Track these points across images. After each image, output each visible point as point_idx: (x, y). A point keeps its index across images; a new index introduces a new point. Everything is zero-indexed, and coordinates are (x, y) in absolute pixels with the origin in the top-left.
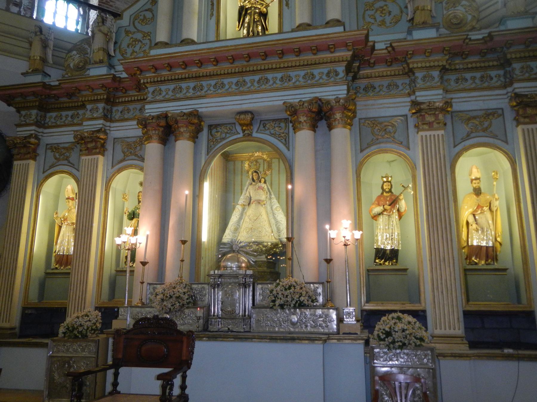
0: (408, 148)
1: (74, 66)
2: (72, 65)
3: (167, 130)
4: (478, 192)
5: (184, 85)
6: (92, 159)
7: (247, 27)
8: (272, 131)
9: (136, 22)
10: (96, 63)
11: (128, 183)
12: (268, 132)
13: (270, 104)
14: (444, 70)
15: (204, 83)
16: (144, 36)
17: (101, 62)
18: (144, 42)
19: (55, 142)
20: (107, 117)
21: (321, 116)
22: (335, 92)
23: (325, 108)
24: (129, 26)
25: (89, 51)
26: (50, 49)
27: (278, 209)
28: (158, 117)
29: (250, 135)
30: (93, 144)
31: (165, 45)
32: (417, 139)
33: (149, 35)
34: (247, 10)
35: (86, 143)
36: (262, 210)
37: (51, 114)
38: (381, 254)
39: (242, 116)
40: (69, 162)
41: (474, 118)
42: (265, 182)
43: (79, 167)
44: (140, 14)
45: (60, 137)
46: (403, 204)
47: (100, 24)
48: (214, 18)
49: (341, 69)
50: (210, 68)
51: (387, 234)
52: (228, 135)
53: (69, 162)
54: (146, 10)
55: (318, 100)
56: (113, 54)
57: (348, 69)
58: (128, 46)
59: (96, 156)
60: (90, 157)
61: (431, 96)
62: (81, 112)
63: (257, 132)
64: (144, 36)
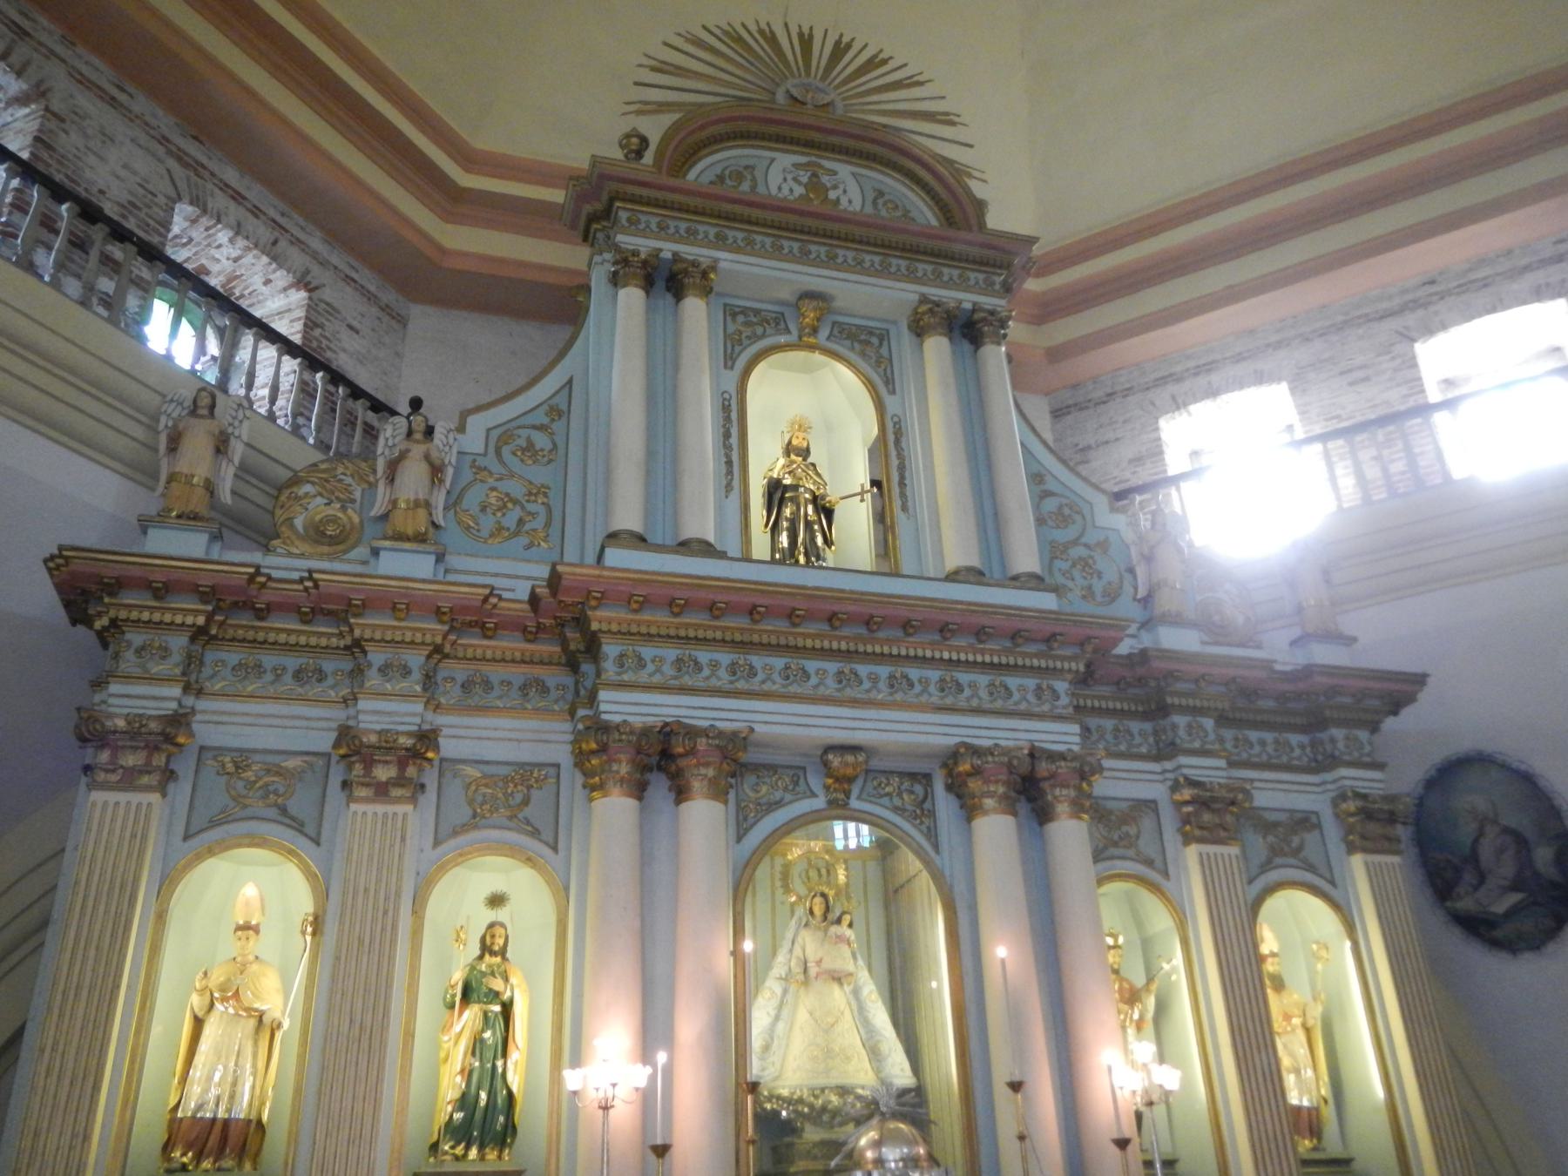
0: (1166, 874)
1: (305, 528)
2: (299, 523)
5: (704, 656)
6: (385, 815)
7: (788, 529)
8: (897, 802)
9: (506, 451)
10: (400, 537)
11: (482, 896)
12: (885, 801)
13: (922, 739)
15: (757, 661)
16: (530, 494)
17: (420, 538)
18: (531, 507)
19: (236, 743)
22: (1061, 736)
23: (1043, 768)
24: (485, 455)
25: (358, 495)
26: (231, 461)
27: (875, 996)
28: (646, 732)
29: (845, 805)
30: (388, 765)
31: (640, 541)
33: (545, 495)
34: (786, 488)
35: (369, 764)
37: (224, 655)
39: (850, 758)
40: (284, 811)
41: (1276, 825)
42: (850, 925)
43: (319, 833)
44: (520, 432)
45: (248, 730)
47: (418, 436)
48: (735, 495)
49: (1061, 686)
50: (773, 627)
52: (788, 797)
53: (284, 811)
54: (534, 427)
56: (440, 521)
58: (483, 509)
59: (402, 809)
60: (380, 809)
62: (328, 666)
63: (859, 798)
64: (530, 494)
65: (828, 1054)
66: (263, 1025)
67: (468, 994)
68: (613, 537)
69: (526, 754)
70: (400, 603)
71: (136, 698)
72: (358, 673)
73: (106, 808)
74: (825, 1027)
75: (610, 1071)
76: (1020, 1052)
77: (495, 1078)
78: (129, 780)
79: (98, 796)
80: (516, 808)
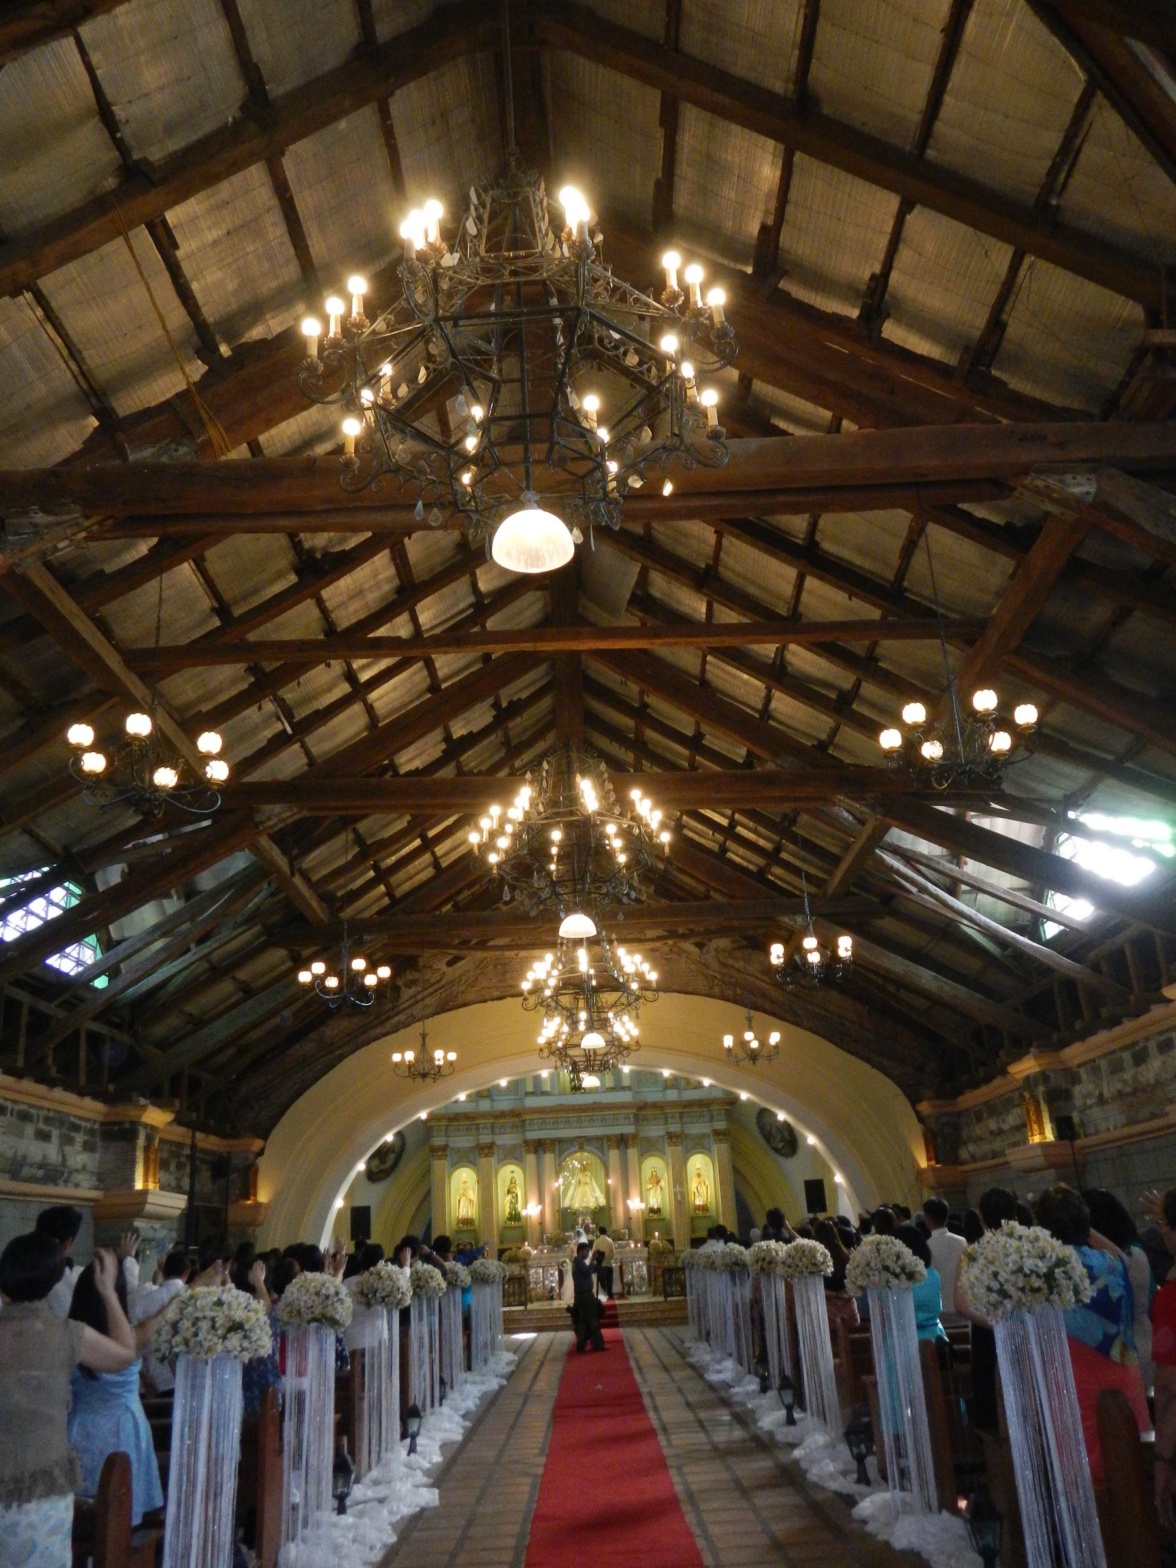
3: (539, 1147)
4: (699, 1175)
11: (509, 1173)
14: (681, 1113)
20: (493, 1133)
21: (622, 1142)
22: (629, 1129)
30: (487, 1150)
31: (533, 1094)
32: (669, 1150)
36: (587, 1187)
38: (652, 1210)
46: (662, 1183)
51: (655, 1200)
55: (622, 1135)
57: (636, 1116)
61: (675, 1128)
65: (582, 1201)
66: (471, 1201)
67: (509, 1192)
68: (527, 1094)
69: (513, 1142)
70: (484, 1115)
71: (438, 1141)
72: (478, 1128)
73: (438, 1165)
74: (584, 1195)
75: (532, 1210)
76: (615, 1199)
77: (515, 1209)
78: (440, 1158)
79: (436, 1162)
80: (513, 1155)
